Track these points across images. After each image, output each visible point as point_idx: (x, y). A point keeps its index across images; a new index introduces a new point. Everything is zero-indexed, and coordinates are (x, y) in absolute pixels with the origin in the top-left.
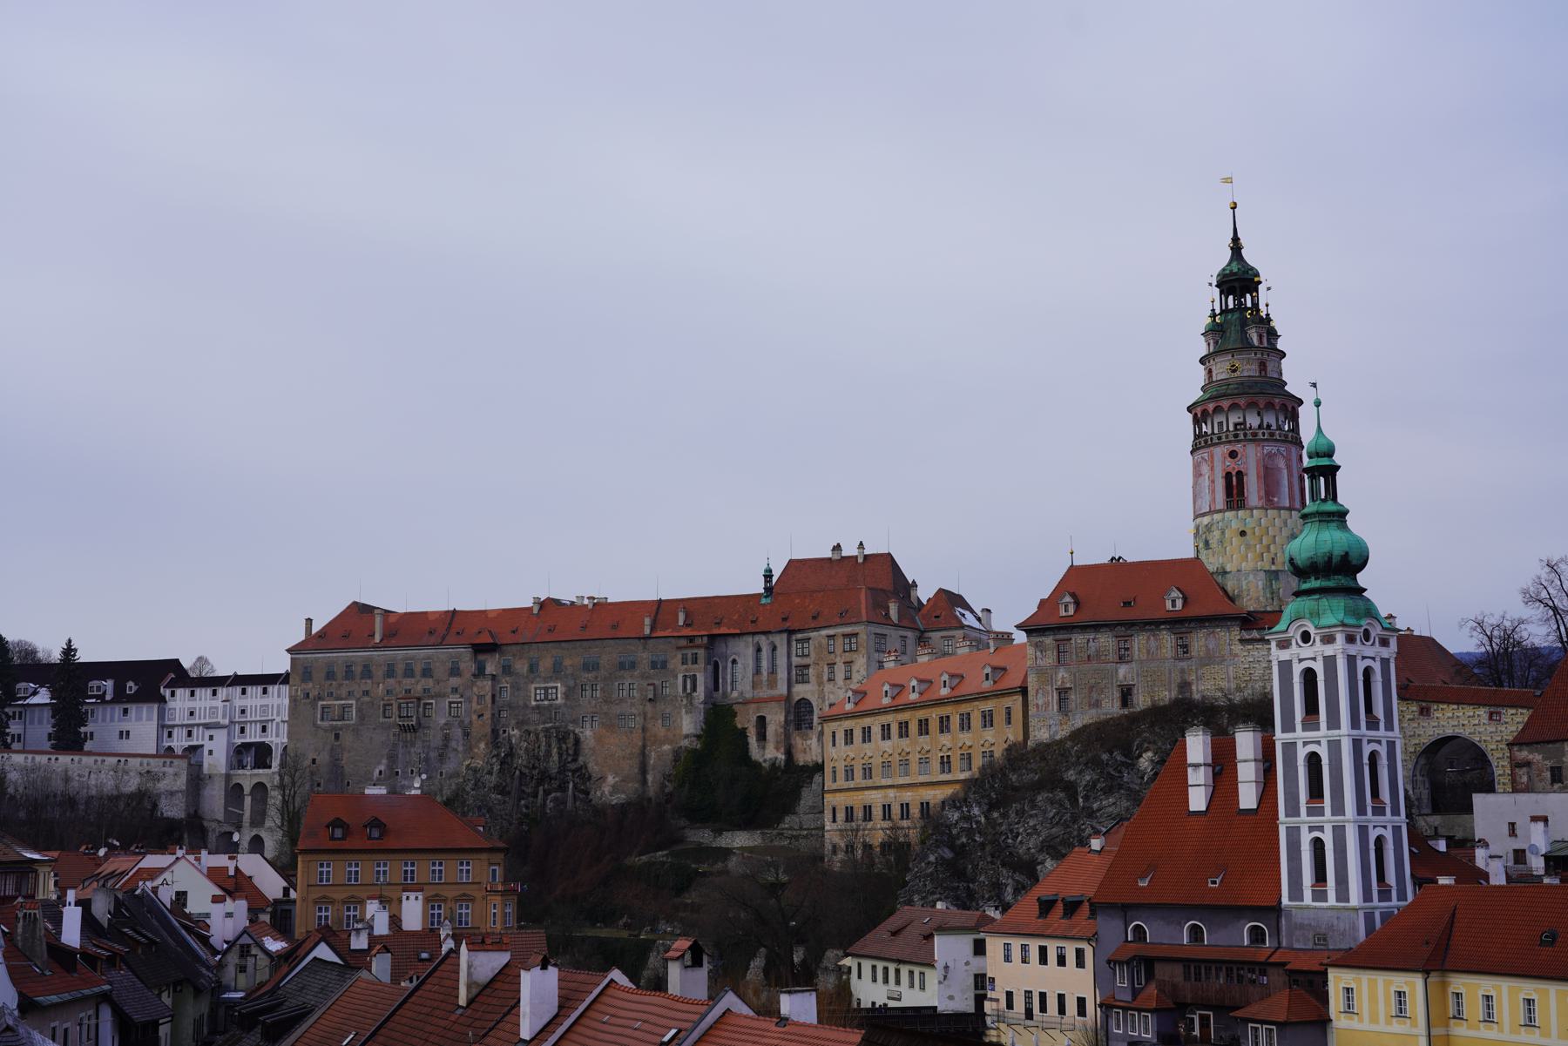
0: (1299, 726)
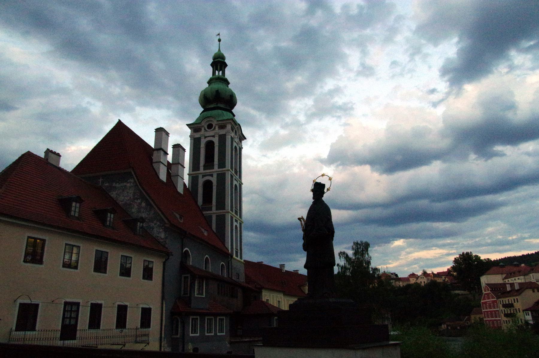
0: (202, 168)
